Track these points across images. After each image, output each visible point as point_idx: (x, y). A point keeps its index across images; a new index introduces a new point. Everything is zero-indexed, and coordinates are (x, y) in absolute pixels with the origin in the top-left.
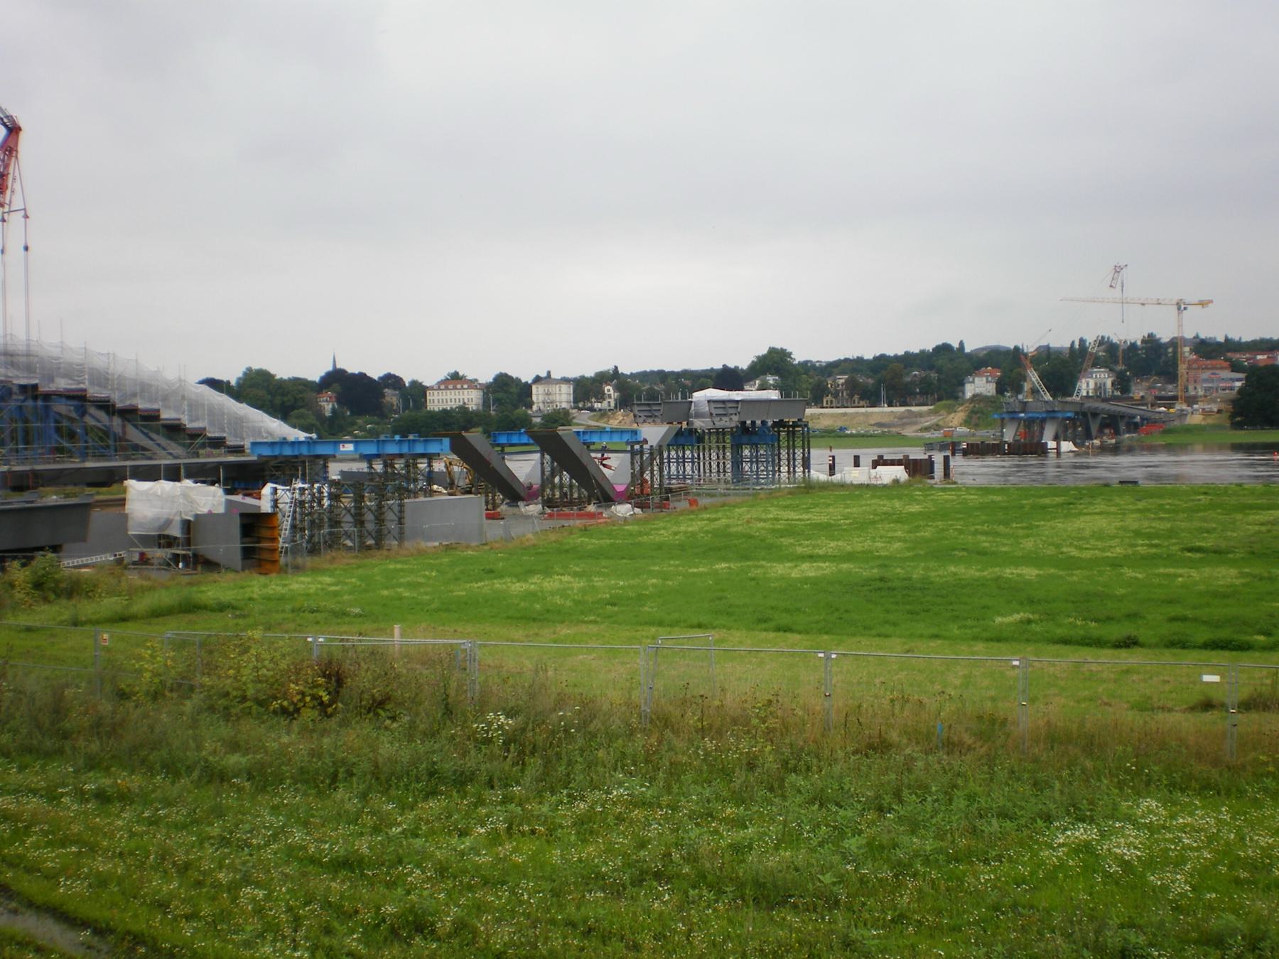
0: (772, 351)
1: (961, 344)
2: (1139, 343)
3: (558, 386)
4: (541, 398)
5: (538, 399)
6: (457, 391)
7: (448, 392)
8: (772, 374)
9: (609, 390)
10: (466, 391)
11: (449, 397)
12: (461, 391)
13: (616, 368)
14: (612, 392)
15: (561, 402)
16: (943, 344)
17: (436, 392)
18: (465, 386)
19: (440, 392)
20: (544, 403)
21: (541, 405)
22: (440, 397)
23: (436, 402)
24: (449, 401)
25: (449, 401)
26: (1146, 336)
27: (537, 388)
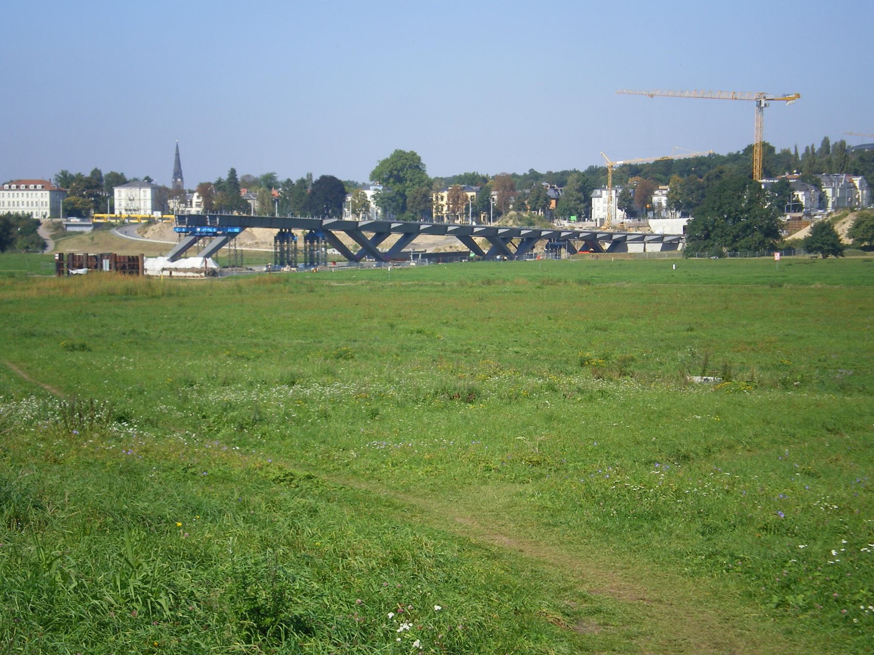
0: (399, 155)
3: (142, 190)
5: (120, 205)
6: (30, 192)
7: (20, 193)
10: (39, 193)
11: (20, 199)
12: (34, 192)
13: (233, 172)
17: (6, 193)
18: (39, 186)
19: (11, 193)
20: (126, 210)
22: (11, 199)
23: (6, 204)
24: (20, 203)
25: (20, 203)
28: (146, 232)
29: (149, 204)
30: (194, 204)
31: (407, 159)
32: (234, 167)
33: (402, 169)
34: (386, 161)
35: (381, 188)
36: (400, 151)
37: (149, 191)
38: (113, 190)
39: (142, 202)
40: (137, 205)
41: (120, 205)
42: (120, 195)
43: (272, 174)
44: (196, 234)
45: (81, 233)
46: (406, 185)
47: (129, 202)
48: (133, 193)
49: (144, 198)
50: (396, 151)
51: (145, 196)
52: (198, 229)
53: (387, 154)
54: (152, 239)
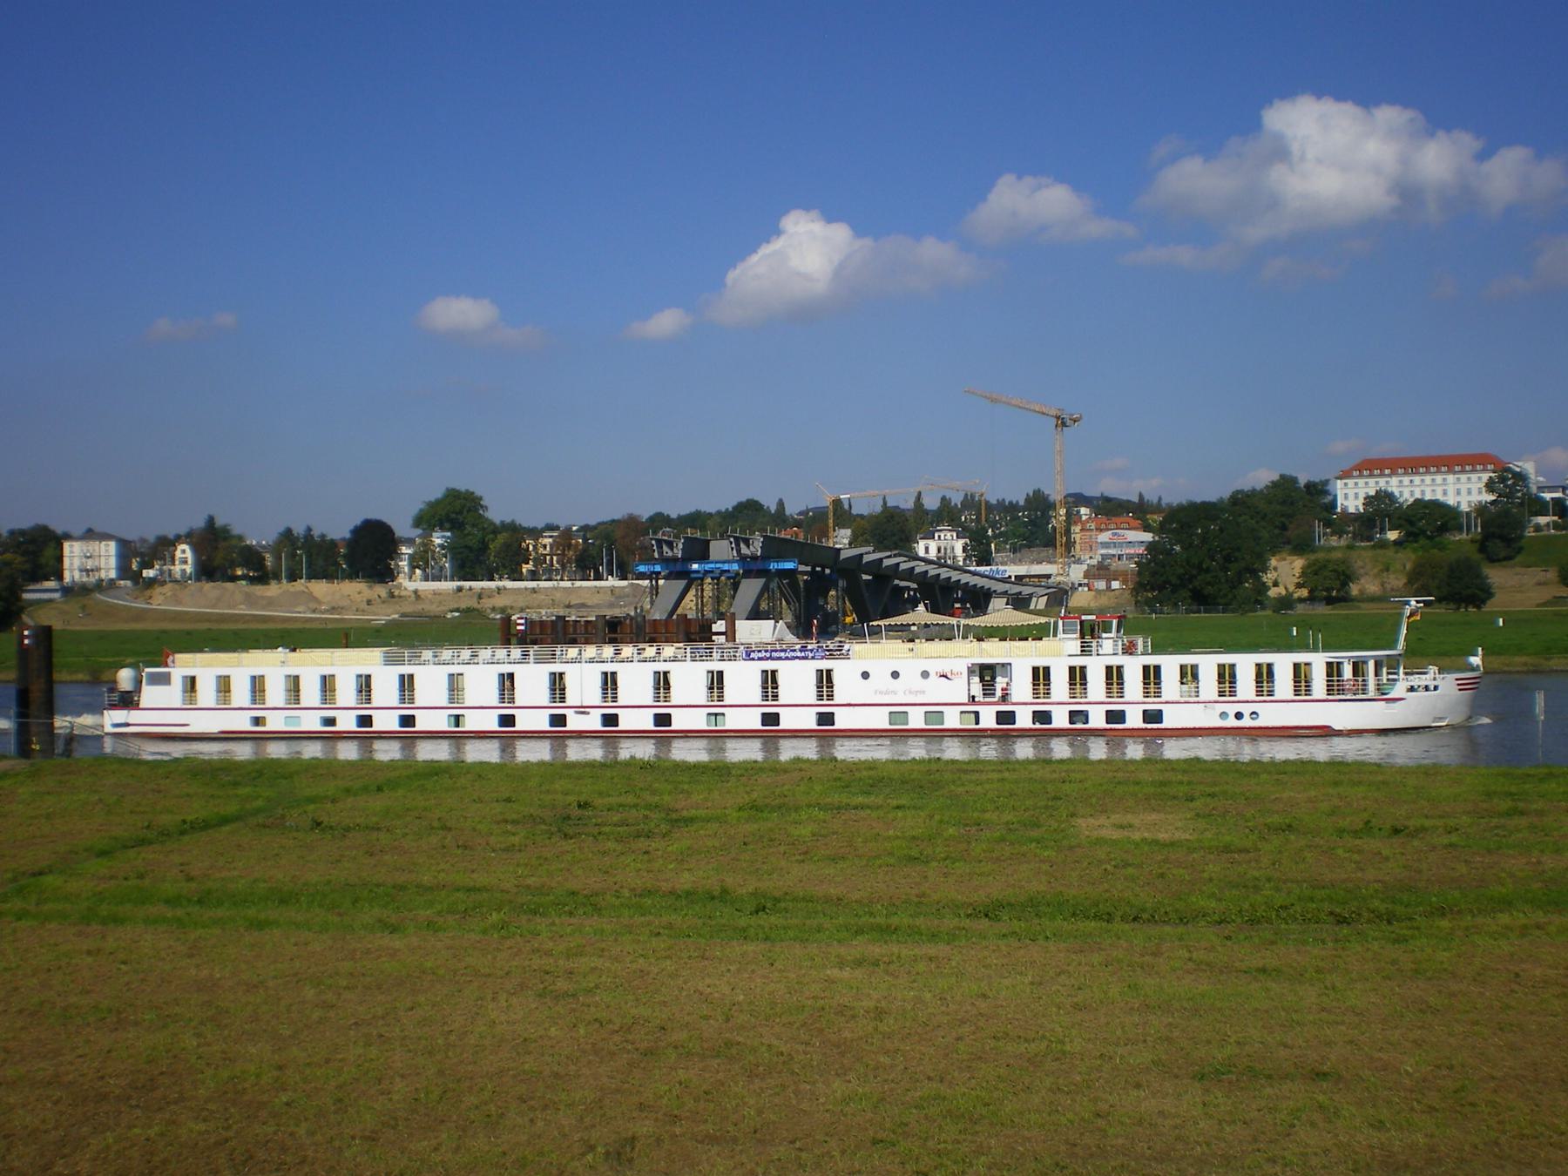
0: (453, 495)
1: (781, 504)
2: (1022, 503)
4: (77, 562)
8: (442, 529)
9: (184, 551)
13: (211, 520)
14: (189, 554)
15: (108, 570)
16: (748, 501)
20: (81, 571)
21: (77, 575)
26: (1031, 494)
27: (71, 546)
28: (151, 597)
29: (113, 562)
30: (177, 562)
31: (464, 498)
32: (211, 513)
33: (460, 513)
34: (438, 502)
35: (449, 534)
36: (453, 489)
37: (112, 546)
38: (62, 544)
39: (103, 559)
40: (97, 563)
41: (72, 564)
42: (72, 552)
43: (226, 526)
44: (693, 575)
45: (51, 601)
46: (466, 532)
47: (84, 560)
48: (90, 548)
49: (107, 558)
50: (448, 489)
51: (107, 551)
52: (695, 566)
53: (437, 493)
54: (165, 605)
